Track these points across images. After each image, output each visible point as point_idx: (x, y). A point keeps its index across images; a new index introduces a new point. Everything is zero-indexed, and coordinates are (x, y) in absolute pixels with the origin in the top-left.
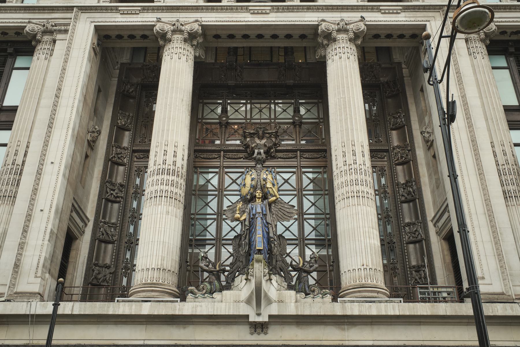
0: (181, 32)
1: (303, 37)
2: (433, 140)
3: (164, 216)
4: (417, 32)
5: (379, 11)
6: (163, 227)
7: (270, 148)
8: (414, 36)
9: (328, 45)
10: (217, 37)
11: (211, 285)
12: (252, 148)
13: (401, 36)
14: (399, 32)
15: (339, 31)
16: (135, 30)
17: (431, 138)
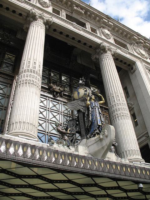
0: (43, 19)
1: (91, 47)
2: (133, 108)
3: (35, 94)
4: (131, 64)
5: (121, 50)
6: (34, 100)
7: (62, 91)
8: (129, 65)
9: (102, 54)
10: (55, 30)
11: (66, 142)
12: (54, 88)
13: (125, 63)
14: (125, 61)
15: (108, 49)
16: (18, 9)
17: (133, 107)
